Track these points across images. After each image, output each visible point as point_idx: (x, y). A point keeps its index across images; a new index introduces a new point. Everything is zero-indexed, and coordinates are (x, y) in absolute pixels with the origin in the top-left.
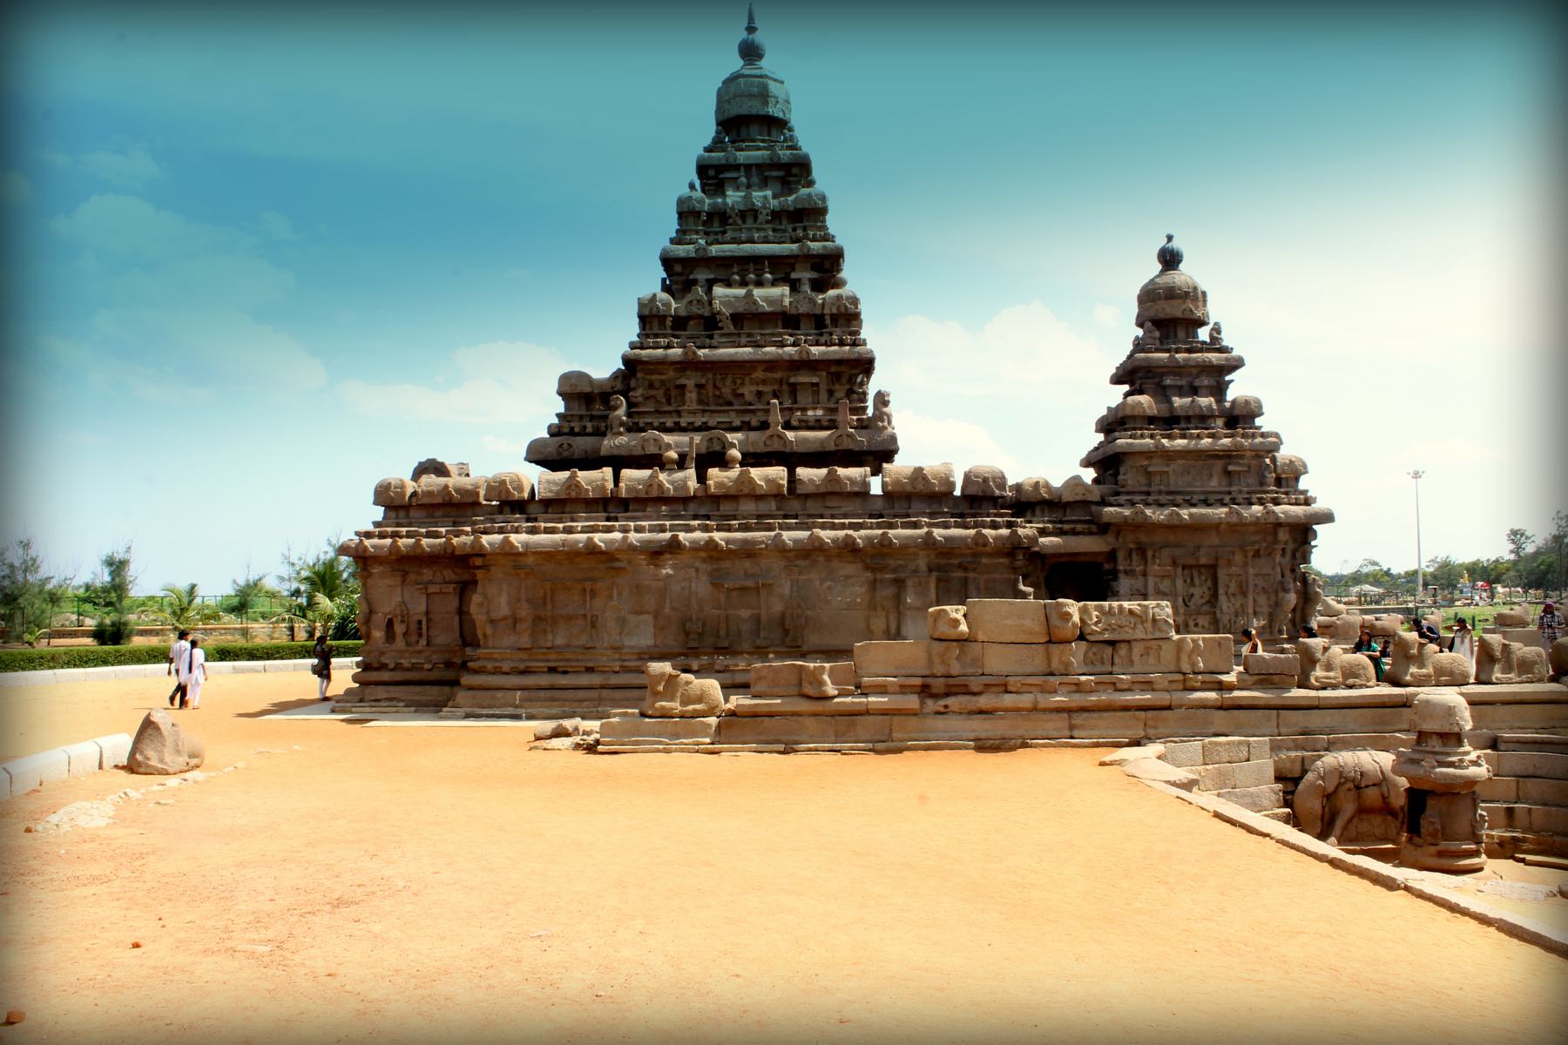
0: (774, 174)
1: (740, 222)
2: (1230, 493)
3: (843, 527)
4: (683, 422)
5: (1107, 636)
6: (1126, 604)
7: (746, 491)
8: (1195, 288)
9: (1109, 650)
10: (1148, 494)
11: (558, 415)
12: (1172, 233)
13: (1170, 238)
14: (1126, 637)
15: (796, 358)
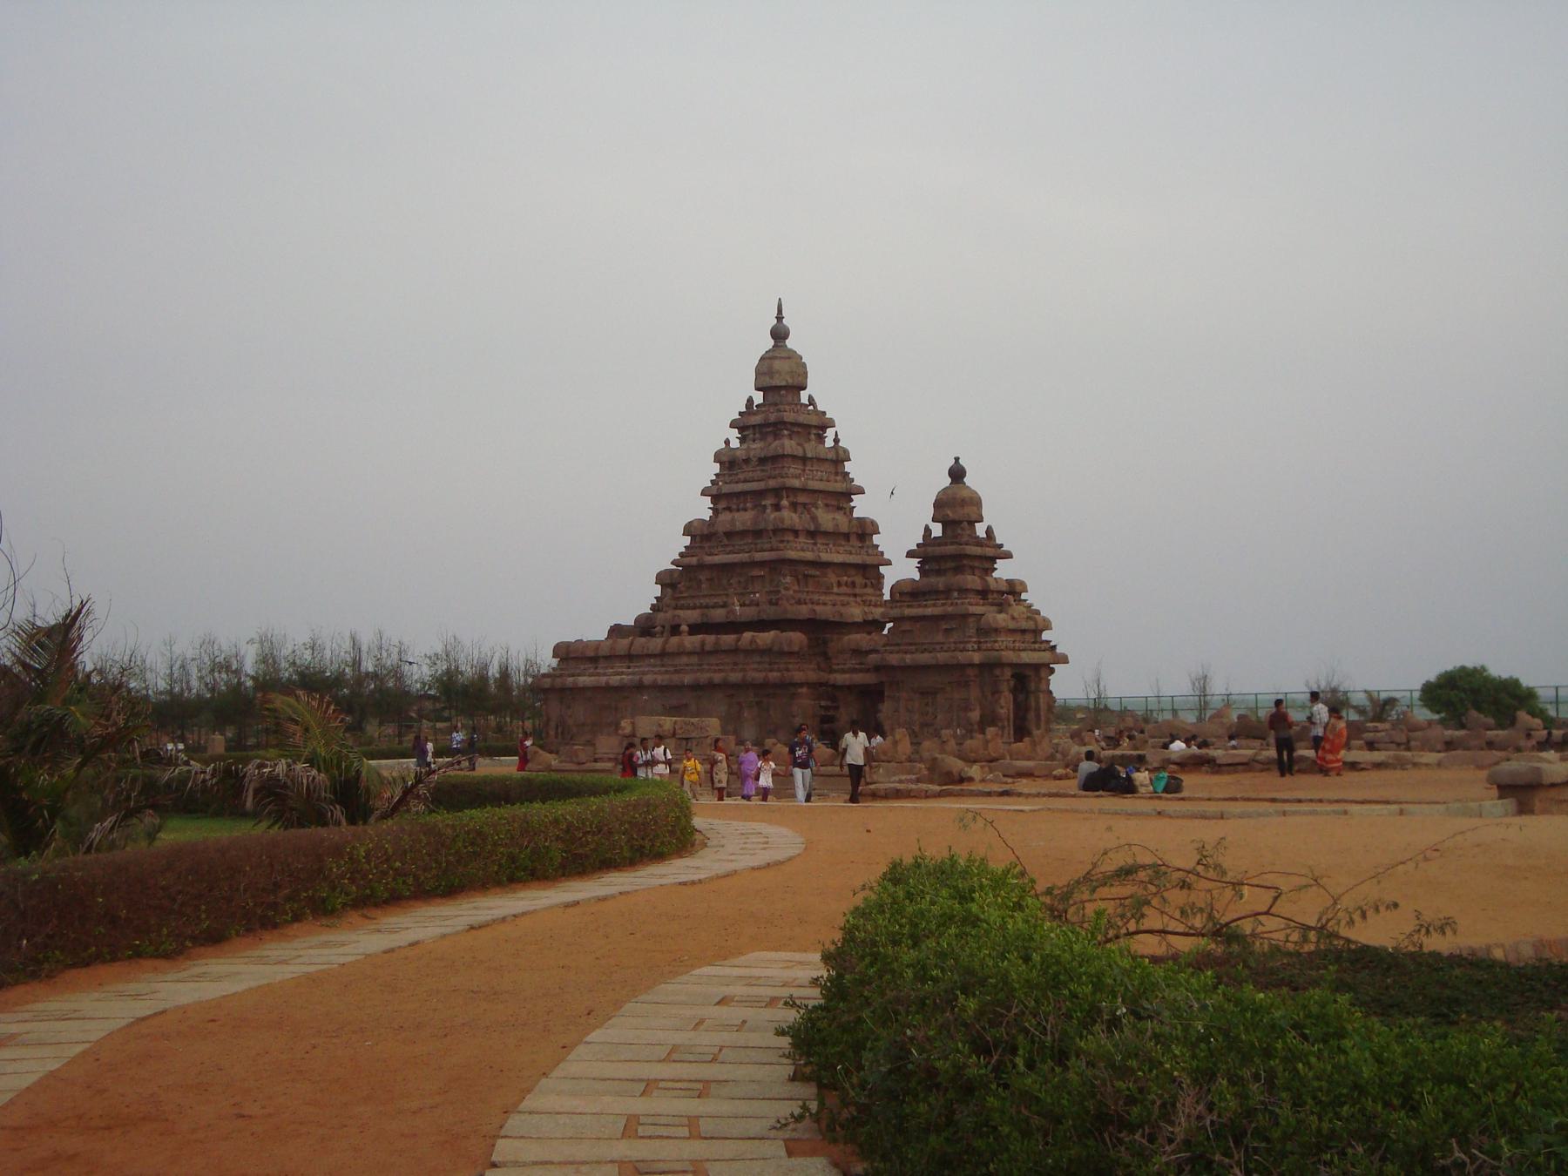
0: (768, 430)
1: (744, 467)
2: (943, 643)
3: (715, 671)
4: (697, 602)
5: (684, 736)
6: (692, 720)
7: (681, 650)
8: (954, 499)
9: (684, 742)
10: (898, 645)
11: (656, 598)
12: (957, 456)
13: (957, 459)
14: (688, 736)
15: (748, 560)
